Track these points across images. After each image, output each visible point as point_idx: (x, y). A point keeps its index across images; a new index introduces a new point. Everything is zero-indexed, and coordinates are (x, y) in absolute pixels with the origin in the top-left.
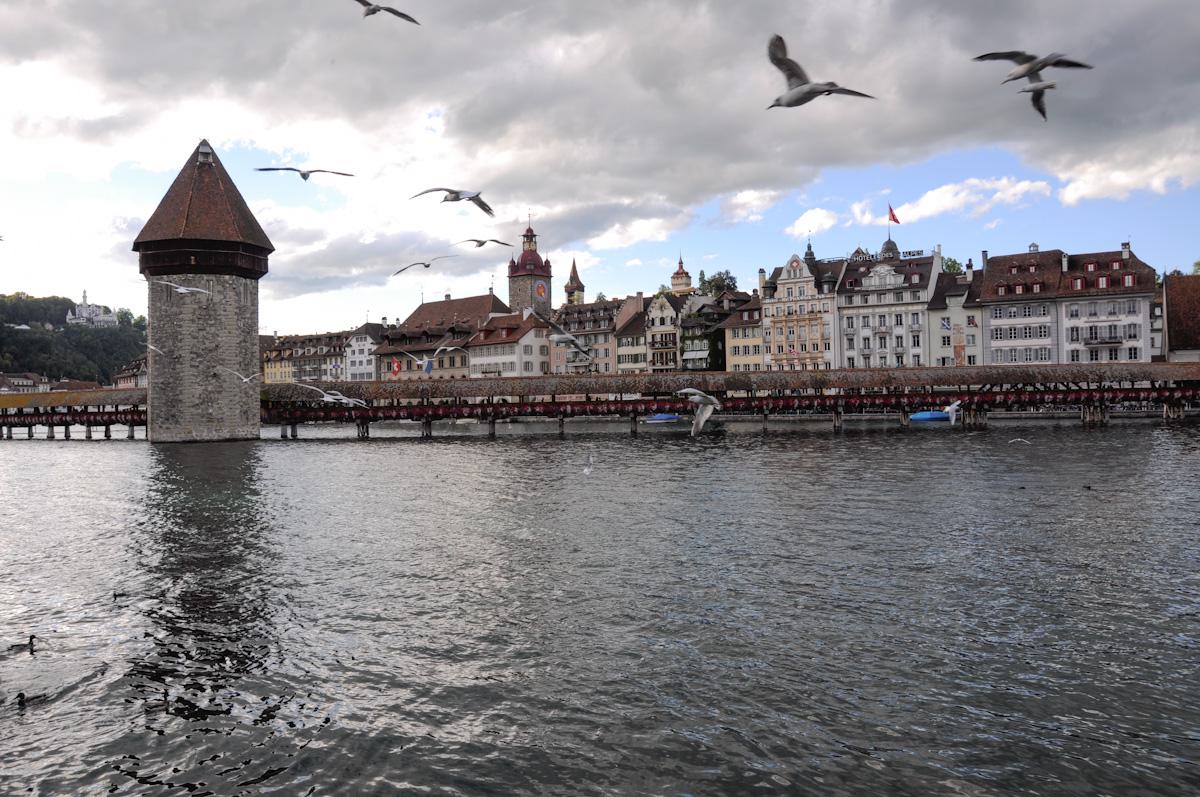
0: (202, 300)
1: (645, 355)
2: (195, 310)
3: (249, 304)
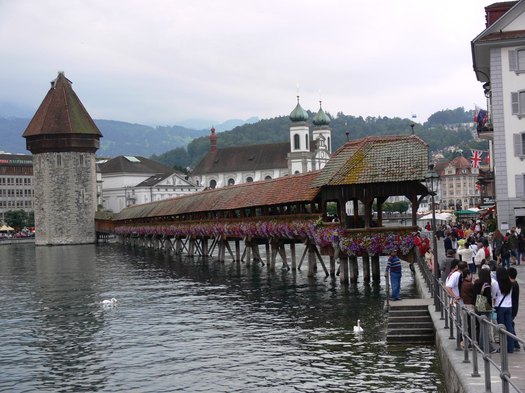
3: (62, 165)
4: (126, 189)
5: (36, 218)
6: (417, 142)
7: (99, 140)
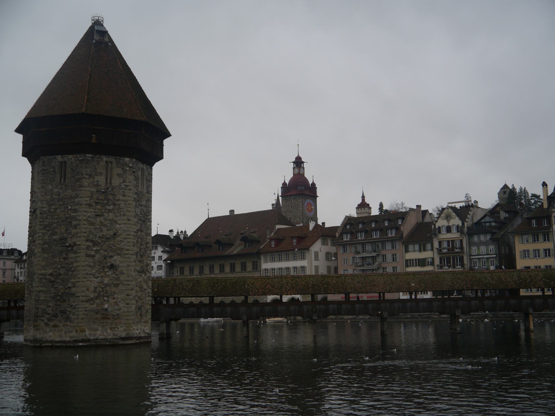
0: (100, 183)
1: (433, 259)
2: (92, 193)
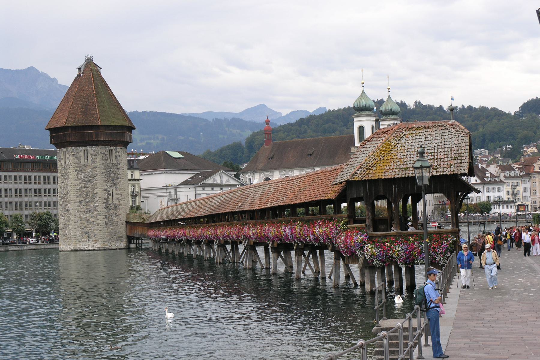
4: (167, 188)
5: (61, 220)
6: (458, 129)
7: (131, 133)
